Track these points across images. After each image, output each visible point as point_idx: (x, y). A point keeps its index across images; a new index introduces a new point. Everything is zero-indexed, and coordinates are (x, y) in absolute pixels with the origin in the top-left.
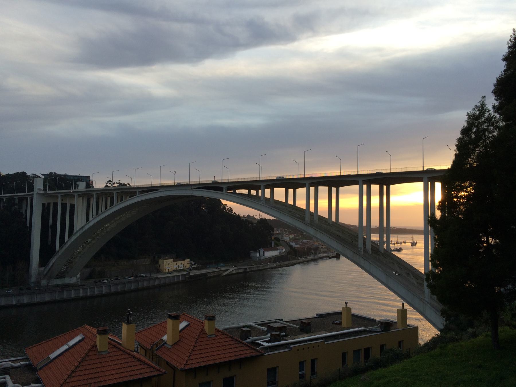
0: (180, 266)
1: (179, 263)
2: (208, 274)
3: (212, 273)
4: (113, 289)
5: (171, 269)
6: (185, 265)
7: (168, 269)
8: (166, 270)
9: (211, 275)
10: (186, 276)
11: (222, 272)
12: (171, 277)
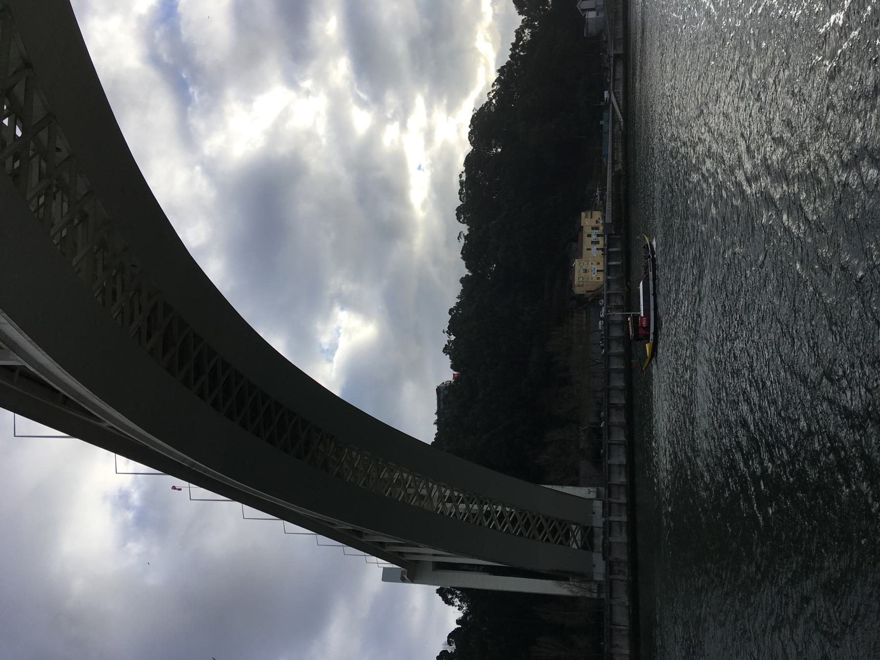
0: (594, 237)
1: (587, 242)
2: (616, 169)
3: (615, 159)
4: (619, 436)
5: (598, 264)
6: (594, 224)
7: (598, 271)
8: (598, 278)
9: (620, 160)
10: (612, 234)
11: (617, 126)
12: (609, 278)
